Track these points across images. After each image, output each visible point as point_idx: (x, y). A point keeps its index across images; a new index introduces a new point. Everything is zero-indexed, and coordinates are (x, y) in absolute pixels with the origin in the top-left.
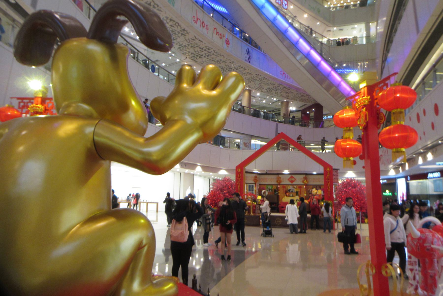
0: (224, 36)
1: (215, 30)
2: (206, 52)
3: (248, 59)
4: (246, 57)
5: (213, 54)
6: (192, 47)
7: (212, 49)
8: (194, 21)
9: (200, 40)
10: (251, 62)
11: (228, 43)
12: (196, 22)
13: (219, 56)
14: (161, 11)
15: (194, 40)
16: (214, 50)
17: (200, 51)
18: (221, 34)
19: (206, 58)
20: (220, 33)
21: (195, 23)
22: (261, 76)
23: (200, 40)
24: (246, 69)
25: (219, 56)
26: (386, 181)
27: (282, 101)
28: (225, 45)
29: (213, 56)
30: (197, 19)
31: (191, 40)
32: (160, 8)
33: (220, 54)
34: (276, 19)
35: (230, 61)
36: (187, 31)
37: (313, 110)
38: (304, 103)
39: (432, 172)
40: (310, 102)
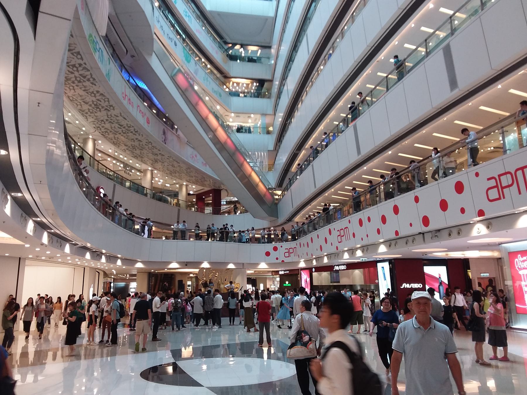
0: (145, 115)
1: (139, 107)
2: (124, 129)
3: (164, 140)
4: (163, 138)
5: (132, 132)
6: (110, 122)
7: (133, 127)
8: (123, 97)
9: (124, 118)
10: (166, 143)
11: (148, 123)
12: (124, 99)
13: (137, 134)
14: (95, 85)
15: (117, 116)
16: (135, 128)
17: (118, 127)
18: (143, 113)
19: (120, 135)
20: (143, 111)
21: (124, 99)
22: (172, 158)
23: (124, 118)
24: (160, 151)
25: (137, 135)
26: (288, 272)
27: (182, 183)
28: (146, 124)
29: (130, 134)
30: (126, 95)
31: (113, 116)
32: (97, 82)
33: (140, 133)
34: (198, 105)
35: (147, 141)
36: (114, 108)
37: (211, 195)
38: (202, 188)
39: (338, 265)
40: (209, 187)
